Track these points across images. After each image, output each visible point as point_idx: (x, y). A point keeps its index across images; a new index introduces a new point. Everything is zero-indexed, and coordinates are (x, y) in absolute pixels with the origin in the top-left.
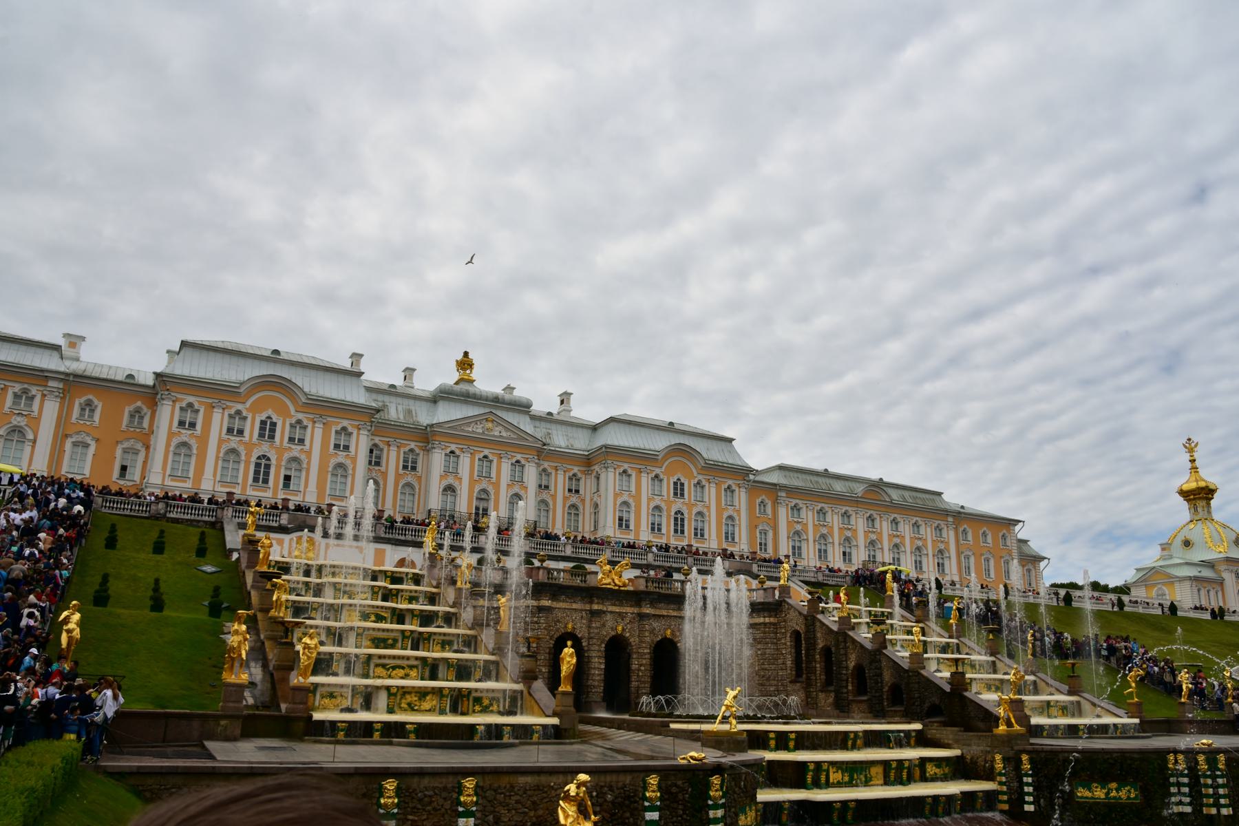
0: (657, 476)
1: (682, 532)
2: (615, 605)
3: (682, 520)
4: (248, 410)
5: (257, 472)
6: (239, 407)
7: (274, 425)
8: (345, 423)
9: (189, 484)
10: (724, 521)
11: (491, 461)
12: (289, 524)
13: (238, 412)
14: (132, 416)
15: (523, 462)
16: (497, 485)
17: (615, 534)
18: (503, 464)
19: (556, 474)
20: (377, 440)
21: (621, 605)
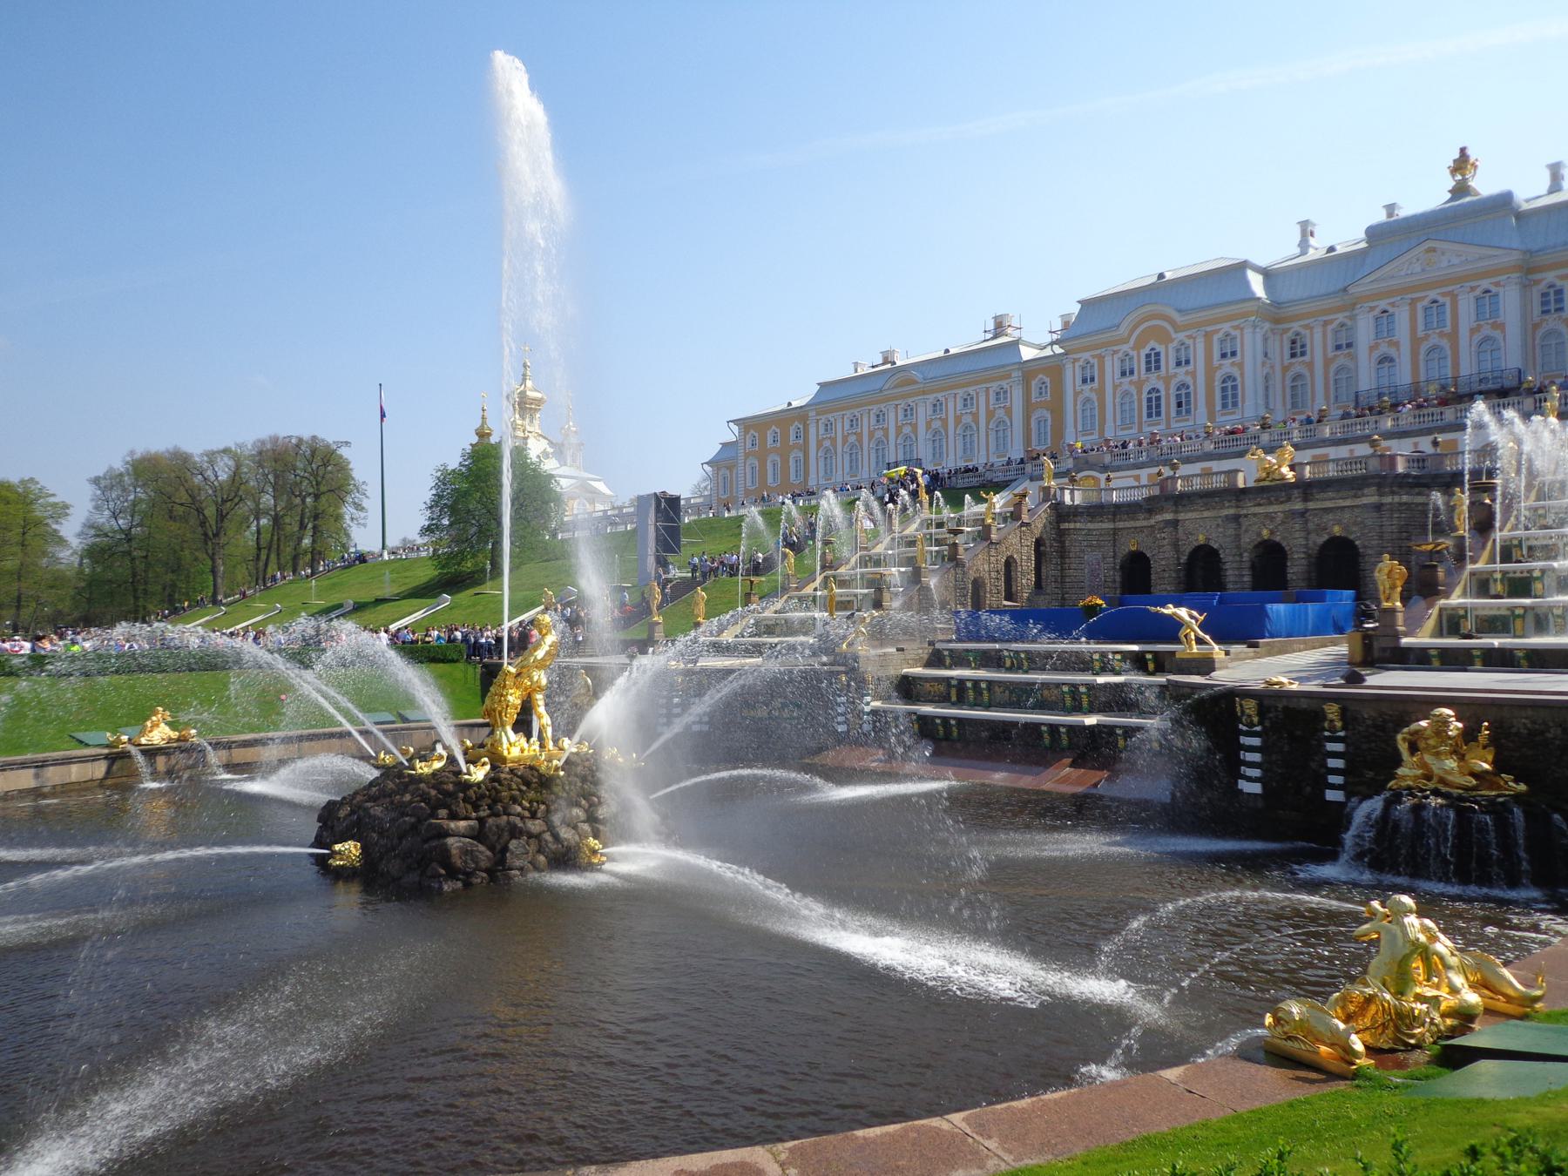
2: (1260, 505)
4: (1133, 349)
5: (1149, 407)
7: (1158, 354)
8: (1226, 327)
9: (1095, 436)
11: (1444, 305)
15: (1494, 289)
16: (1454, 336)
18: (1460, 302)
21: (1271, 503)
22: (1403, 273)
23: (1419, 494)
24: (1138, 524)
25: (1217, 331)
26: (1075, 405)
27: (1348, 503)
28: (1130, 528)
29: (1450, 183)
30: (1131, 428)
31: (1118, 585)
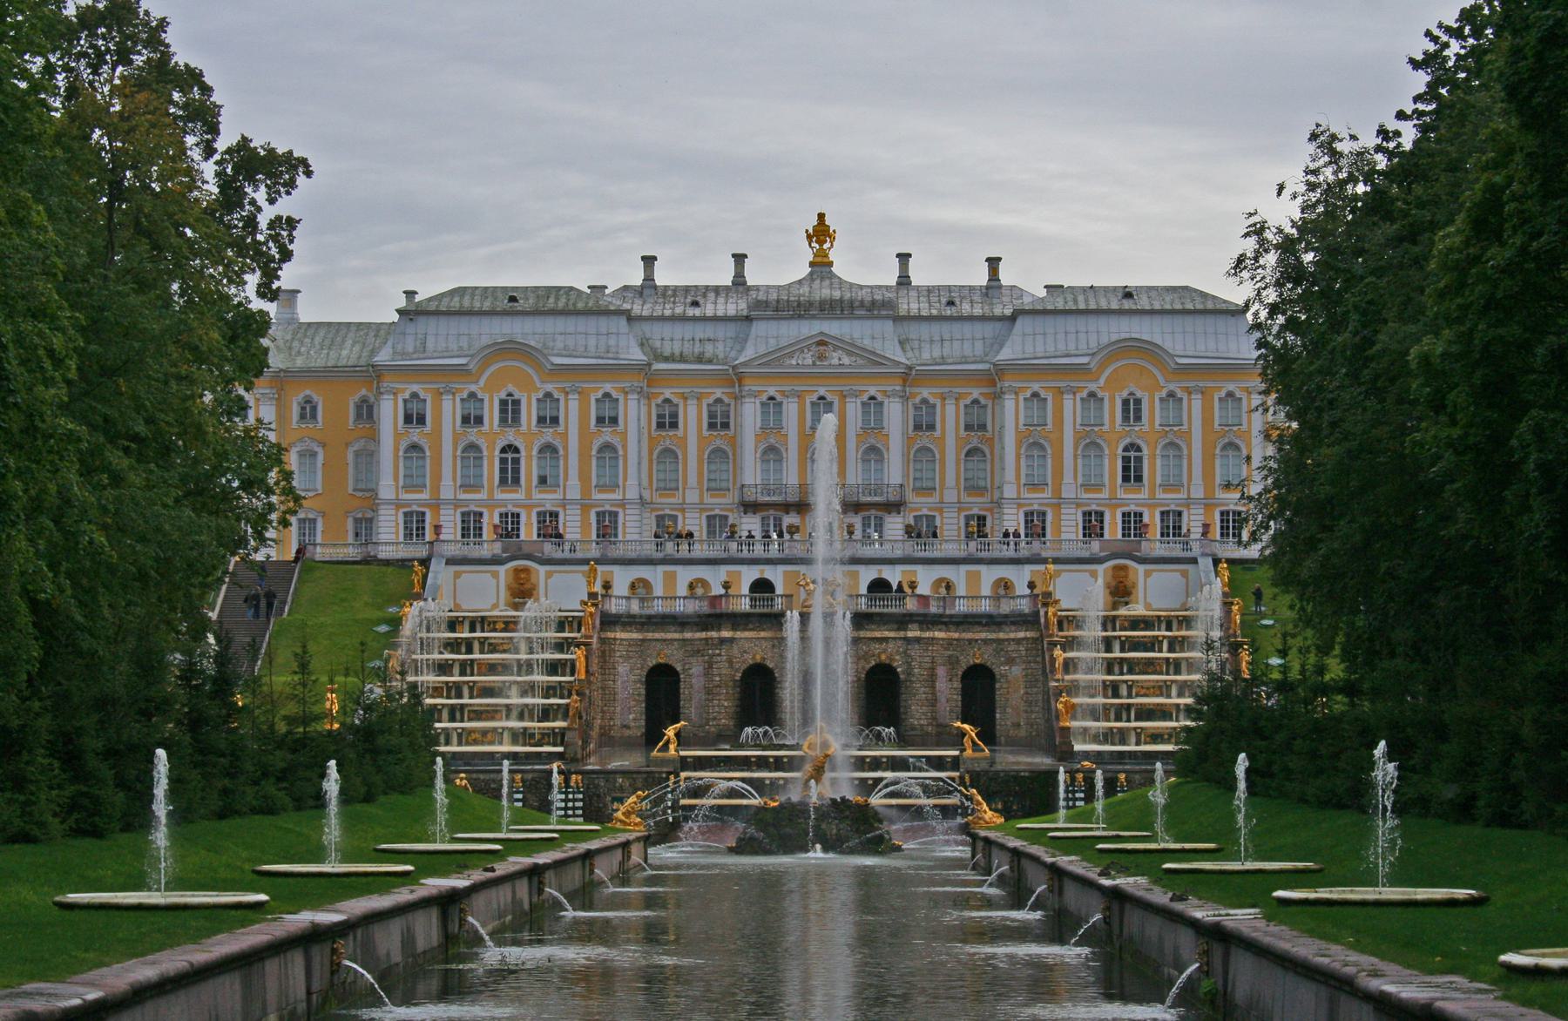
0: (1092, 395)
1: (1139, 479)
3: (1139, 460)
5: (503, 470)
6: (473, 388)
7: (517, 403)
8: (608, 387)
10: (1218, 451)
12: (504, 552)
13: (472, 395)
14: (359, 407)
15: (880, 397)
17: (1019, 492)
19: (943, 406)
20: (668, 393)
22: (794, 362)
23: (940, 630)
24: (670, 636)
25: (597, 389)
26: (397, 449)
27: (892, 634)
28: (657, 640)
29: (809, 256)
30: (479, 492)
31: (643, 698)
